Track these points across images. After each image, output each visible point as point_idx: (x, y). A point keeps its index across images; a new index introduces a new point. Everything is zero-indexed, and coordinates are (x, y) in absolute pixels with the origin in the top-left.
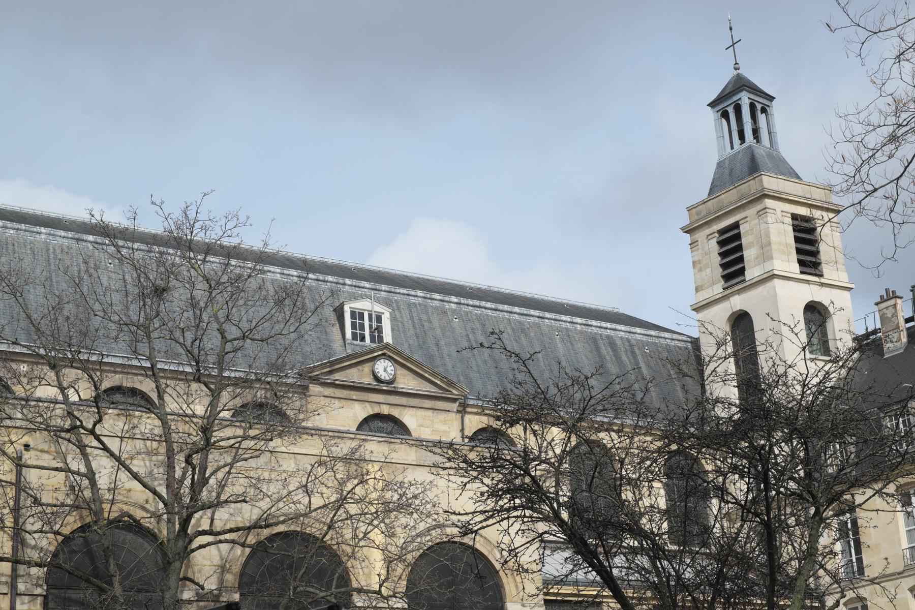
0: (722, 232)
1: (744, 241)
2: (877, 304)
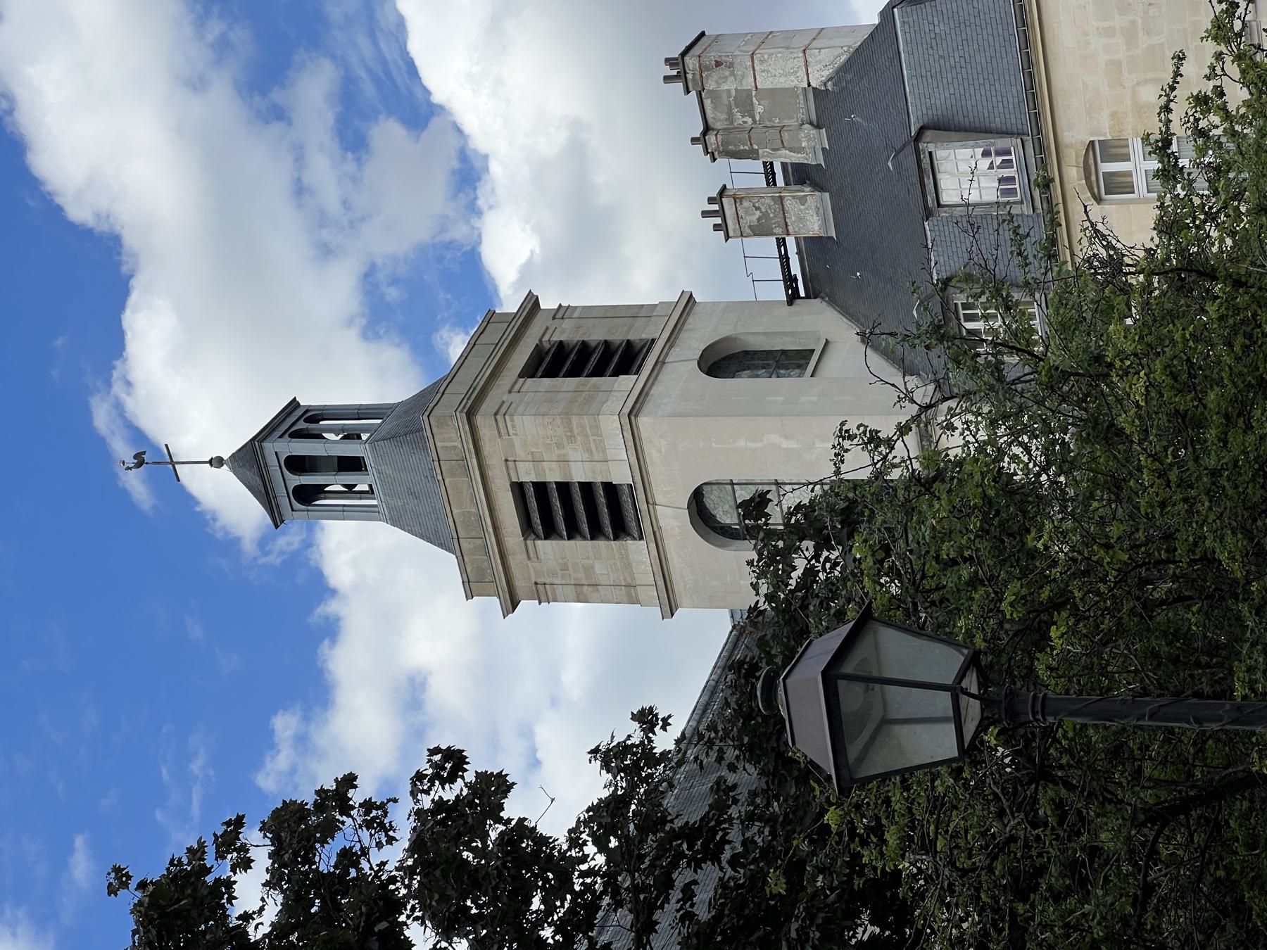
0: (527, 528)
1: (553, 476)
2: (727, 237)
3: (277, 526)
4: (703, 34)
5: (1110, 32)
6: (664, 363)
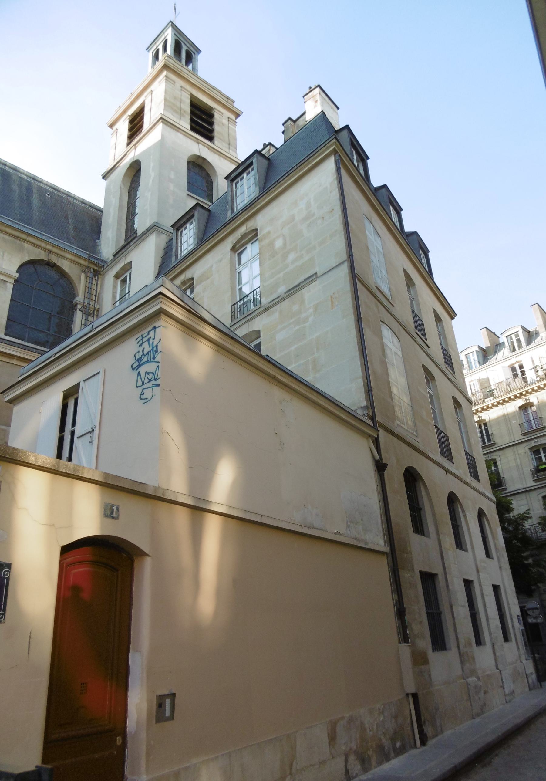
3: (147, 49)
4: (338, 108)
5: (308, 205)
6: (198, 143)
